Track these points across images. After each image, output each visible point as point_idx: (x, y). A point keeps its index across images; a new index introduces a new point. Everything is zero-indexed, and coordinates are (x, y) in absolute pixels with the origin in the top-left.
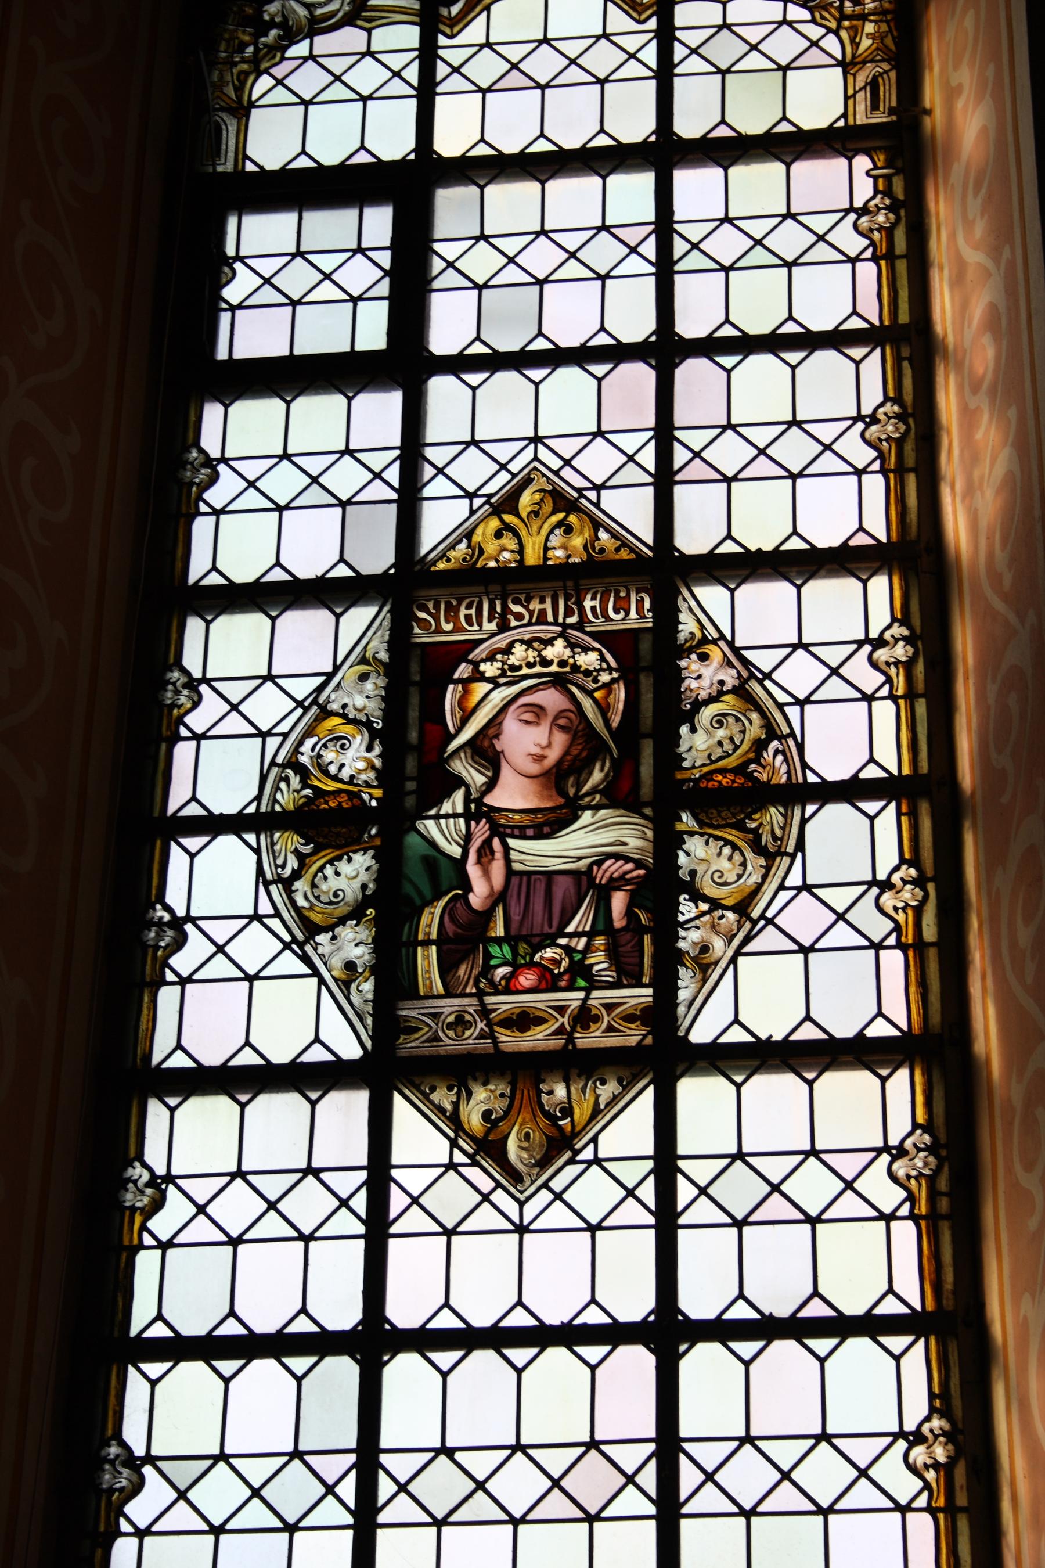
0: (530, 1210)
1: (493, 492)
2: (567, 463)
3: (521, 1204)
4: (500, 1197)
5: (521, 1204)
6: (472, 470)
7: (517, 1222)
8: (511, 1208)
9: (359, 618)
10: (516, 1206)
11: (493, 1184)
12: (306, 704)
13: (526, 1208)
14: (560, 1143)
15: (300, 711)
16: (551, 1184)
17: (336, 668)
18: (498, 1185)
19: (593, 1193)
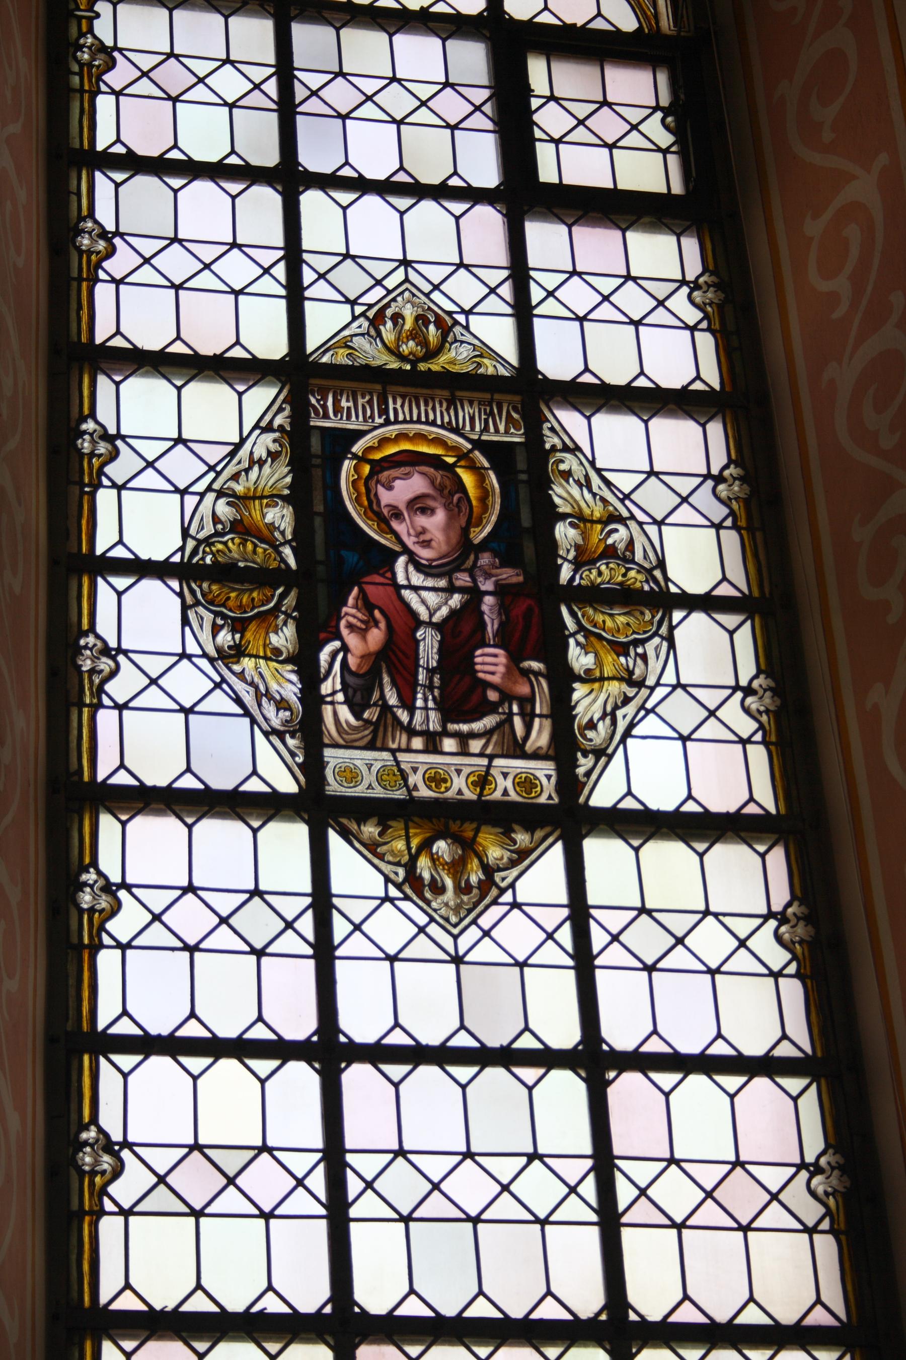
0: (464, 943)
1: (373, 302)
2: (436, 287)
3: (455, 938)
4: (433, 929)
5: (455, 938)
6: (351, 279)
7: (453, 952)
8: (447, 942)
9: (261, 397)
10: (451, 940)
11: (427, 919)
12: (219, 468)
13: (460, 940)
14: (489, 888)
15: (212, 475)
16: (480, 921)
17: (243, 441)
18: (474, 922)
19: (517, 934)
